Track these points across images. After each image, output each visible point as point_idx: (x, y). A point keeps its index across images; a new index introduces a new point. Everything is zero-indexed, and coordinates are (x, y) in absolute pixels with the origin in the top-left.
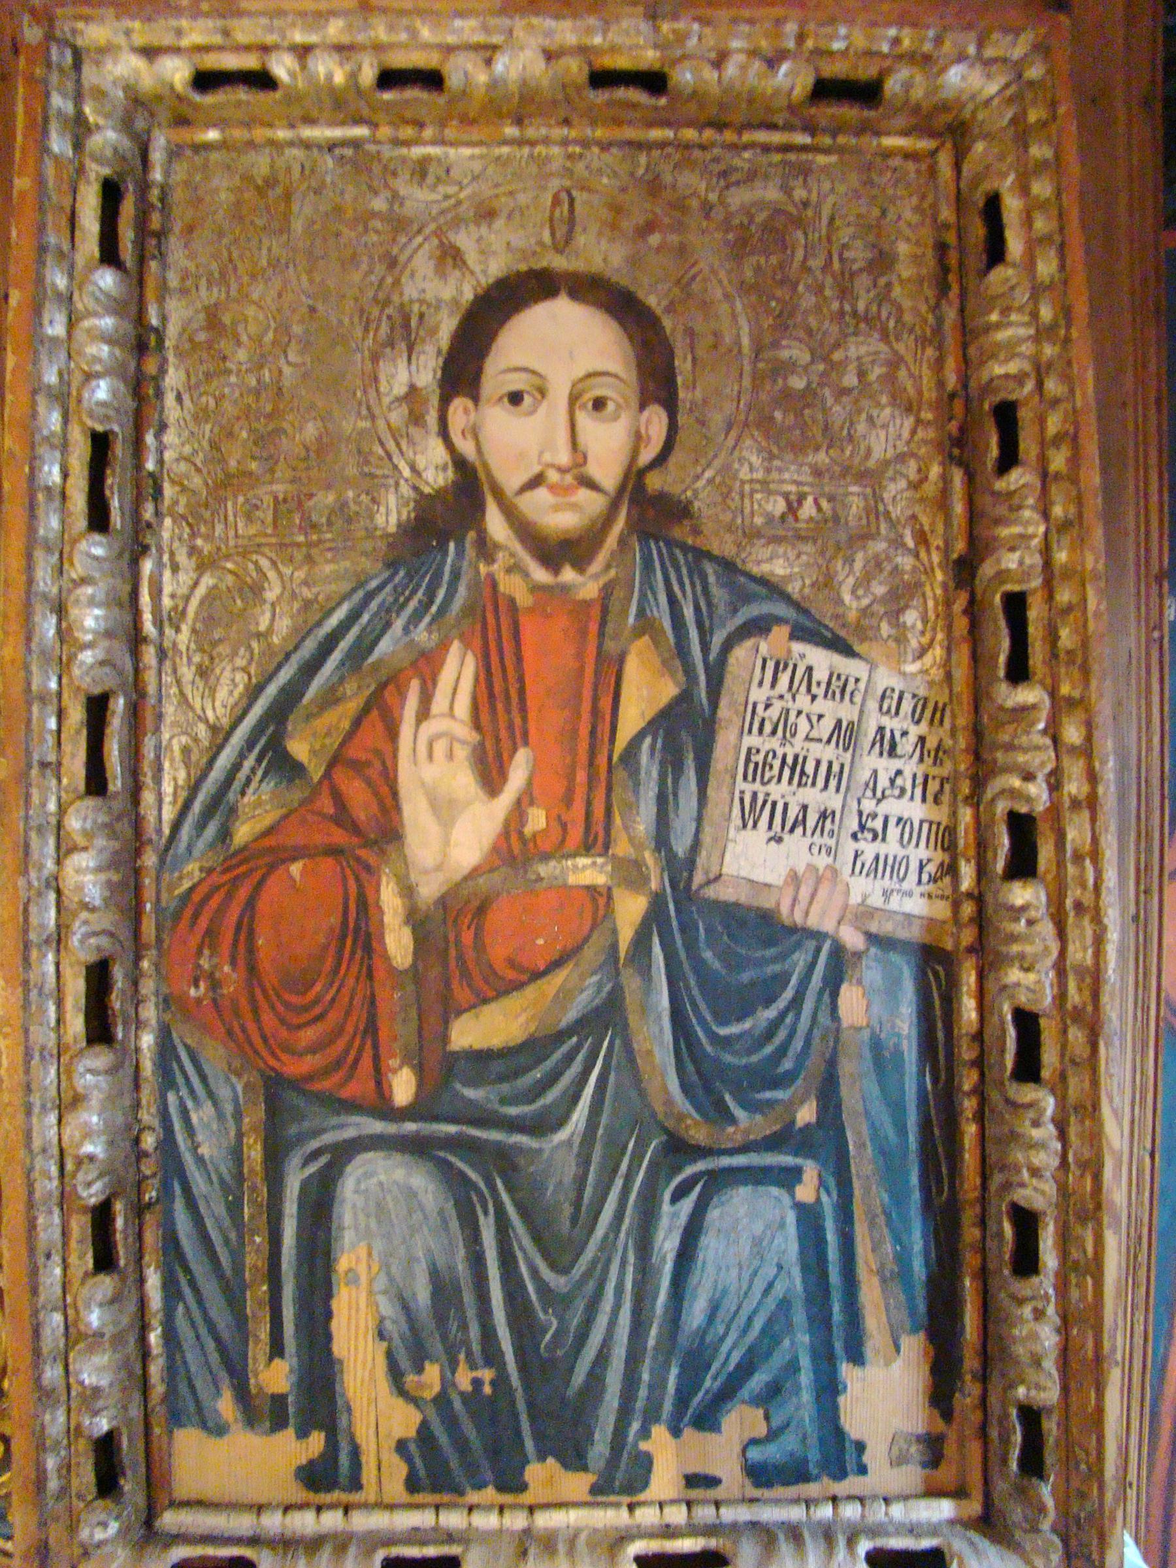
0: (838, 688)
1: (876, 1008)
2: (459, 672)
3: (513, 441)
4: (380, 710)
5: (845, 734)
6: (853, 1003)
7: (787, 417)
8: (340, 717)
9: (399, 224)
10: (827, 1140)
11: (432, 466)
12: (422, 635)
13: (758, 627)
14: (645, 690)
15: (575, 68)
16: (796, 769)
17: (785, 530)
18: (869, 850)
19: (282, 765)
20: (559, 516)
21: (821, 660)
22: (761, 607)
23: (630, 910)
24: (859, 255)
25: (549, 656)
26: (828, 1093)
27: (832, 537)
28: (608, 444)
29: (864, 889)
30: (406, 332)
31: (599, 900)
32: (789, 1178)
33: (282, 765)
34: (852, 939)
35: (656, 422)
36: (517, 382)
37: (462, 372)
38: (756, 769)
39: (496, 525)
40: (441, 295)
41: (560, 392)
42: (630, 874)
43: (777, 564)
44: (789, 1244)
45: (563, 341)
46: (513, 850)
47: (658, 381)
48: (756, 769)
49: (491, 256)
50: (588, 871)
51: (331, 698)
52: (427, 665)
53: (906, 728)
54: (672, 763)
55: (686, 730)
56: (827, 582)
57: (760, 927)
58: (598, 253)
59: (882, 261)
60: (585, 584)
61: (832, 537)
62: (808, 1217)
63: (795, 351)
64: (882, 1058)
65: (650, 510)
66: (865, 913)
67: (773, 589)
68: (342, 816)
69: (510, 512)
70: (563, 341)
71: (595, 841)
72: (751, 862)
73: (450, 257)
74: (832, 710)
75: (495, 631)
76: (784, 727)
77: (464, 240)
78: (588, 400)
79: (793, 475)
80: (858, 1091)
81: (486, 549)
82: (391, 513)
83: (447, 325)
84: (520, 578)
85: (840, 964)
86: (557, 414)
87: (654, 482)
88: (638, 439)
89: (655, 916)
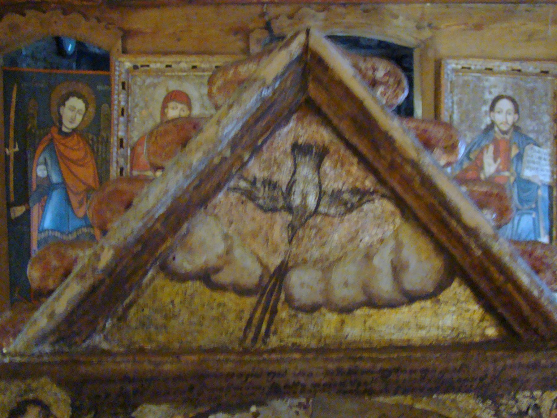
0: (539, 152)
1: (543, 193)
2: (491, 148)
3: (499, 118)
4: (482, 152)
5: (540, 158)
6: (540, 192)
7: (533, 116)
8: (477, 153)
9: (484, 88)
10: (536, 209)
11: (488, 121)
12: (487, 143)
13: (529, 144)
14: (514, 152)
15: (510, 69)
16: (534, 162)
17: (532, 131)
18: (542, 173)
19: (469, 159)
20: (504, 128)
21: (536, 148)
22: (528, 141)
23: (512, 179)
24: (544, 94)
25: (503, 147)
26: (536, 203)
27: (539, 132)
28: (511, 119)
29: (541, 178)
30: (485, 102)
31: (508, 178)
32: (531, 214)
33: (469, 159)
34: (540, 184)
35: (516, 116)
36: (499, 110)
37: (492, 108)
38: (528, 162)
39: (496, 129)
40: (489, 97)
41: (504, 112)
42: (512, 174)
43: (532, 136)
44: (531, 222)
45: (505, 105)
46: (498, 171)
47: (517, 111)
48: (528, 162)
49: (496, 92)
50: (507, 174)
51: (475, 150)
52: (487, 147)
53: (548, 158)
54: (518, 161)
55: (520, 156)
56: (538, 138)
57: (528, 182)
58: (509, 93)
59: (546, 95)
60: (507, 137)
61: (539, 132)
62: (534, 219)
63: (534, 107)
64: (543, 199)
65: (516, 128)
66: (541, 181)
67: (530, 139)
68: (476, 165)
69: (498, 128)
70: (505, 105)
71: (508, 170)
72: (527, 173)
73: (490, 93)
74: (538, 155)
75: (496, 142)
76: (532, 156)
77: (492, 90)
78: (508, 113)
79: (534, 124)
80: (540, 204)
81: (495, 132)
82: (483, 127)
83: (490, 103)
84: (499, 136)
85: (538, 187)
86: (504, 115)
87: (517, 124)
88: (514, 118)
89: (515, 180)
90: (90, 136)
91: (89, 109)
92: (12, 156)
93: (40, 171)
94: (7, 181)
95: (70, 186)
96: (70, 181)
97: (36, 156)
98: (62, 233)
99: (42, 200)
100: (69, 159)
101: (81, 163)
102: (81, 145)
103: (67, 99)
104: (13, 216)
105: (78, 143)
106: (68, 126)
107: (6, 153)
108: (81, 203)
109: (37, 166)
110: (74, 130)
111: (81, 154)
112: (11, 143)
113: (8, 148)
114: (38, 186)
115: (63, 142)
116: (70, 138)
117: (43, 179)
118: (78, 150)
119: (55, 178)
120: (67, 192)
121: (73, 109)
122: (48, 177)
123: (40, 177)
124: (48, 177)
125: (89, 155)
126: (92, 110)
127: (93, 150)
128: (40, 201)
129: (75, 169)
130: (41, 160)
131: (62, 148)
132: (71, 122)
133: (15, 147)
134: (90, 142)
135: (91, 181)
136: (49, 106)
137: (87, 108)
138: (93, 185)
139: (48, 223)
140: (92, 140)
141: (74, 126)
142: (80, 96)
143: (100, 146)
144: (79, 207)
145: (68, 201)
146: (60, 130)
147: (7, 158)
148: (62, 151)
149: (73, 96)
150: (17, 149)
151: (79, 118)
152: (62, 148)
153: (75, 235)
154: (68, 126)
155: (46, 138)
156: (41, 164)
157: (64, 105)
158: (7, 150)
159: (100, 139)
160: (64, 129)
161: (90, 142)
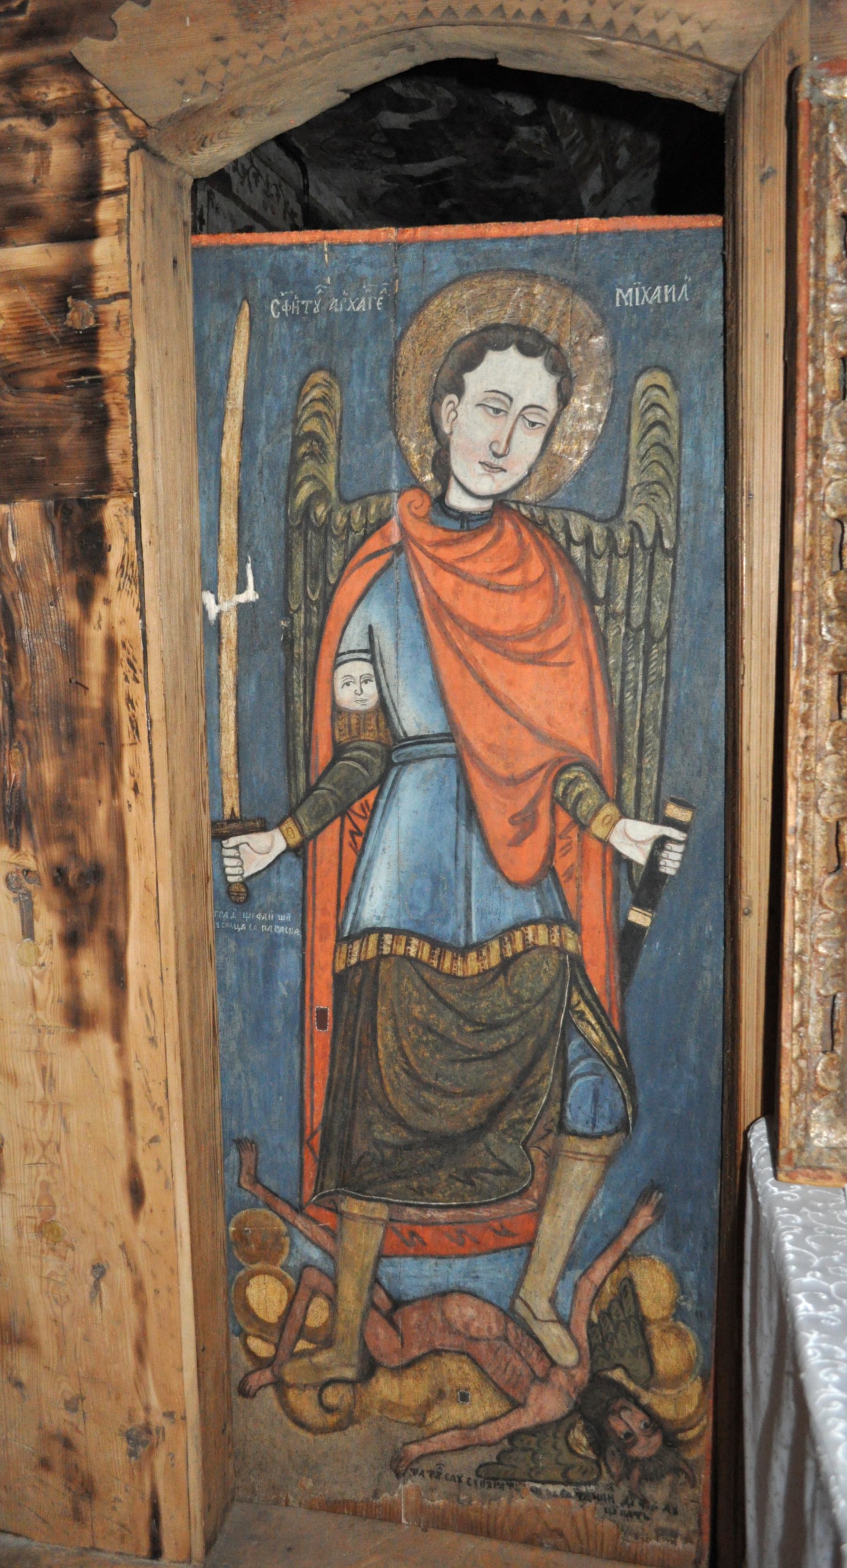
90: (577, 526)
91: (575, 401)
92: (230, 627)
93: (352, 688)
94: (212, 727)
95: (478, 747)
96: (479, 727)
97: (332, 627)
98: (435, 943)
99: (356, 807)
100: (480, 635)
101: (530, 647)
102: (536, 568)
103: (472, 361)
104: (234, 872)
105: (520, 562)
106: (474, 483)
107: (205, 613)
108: (525, 822)
109: (336, 666)
110: (501, 503)
111: (535, 608)
112: (227, 568)
113: (214, 592)
114: (339, 751)
115: (447, 554)
116: (488, 538)
117: (362, 716)
118: (523, 588)
119: (414, 716)
120: (463, 779)
121: (498, 404)
122: (383, 707)
123: (350, 713)
124: (383, 707)
125: (570, 613)
126: (588, 404)
127: (589, 587)
128: (344, 812)
129: (498, 671)
130: (355, 638)
131: (445, 583)
132: (491, 468)
133: (241, 588)
134: (578, 552)
135: (575, 732)
136: (392, 400)
137: (563, 399)
138: (584, 744)
139: (376, 904)
140: (587, 541)
141: (501, 483)
142: (532, 344)
143: (623, 565)
144: (517, 842)
145: (469, 810)
146: (440, 501)
147: (213, 631)
148: (447, 597)
149: (501, 347)
150: (250, 595)
151: (527, 445)
152: (445, 583)
153: (494, 960)
154: (474, 483)
155: (374, 543)
156: (355, 655)
157: (459, 390)
158: (208, 598)
159: (623, 538)
160: (457, 499)
161: (578, 552)
